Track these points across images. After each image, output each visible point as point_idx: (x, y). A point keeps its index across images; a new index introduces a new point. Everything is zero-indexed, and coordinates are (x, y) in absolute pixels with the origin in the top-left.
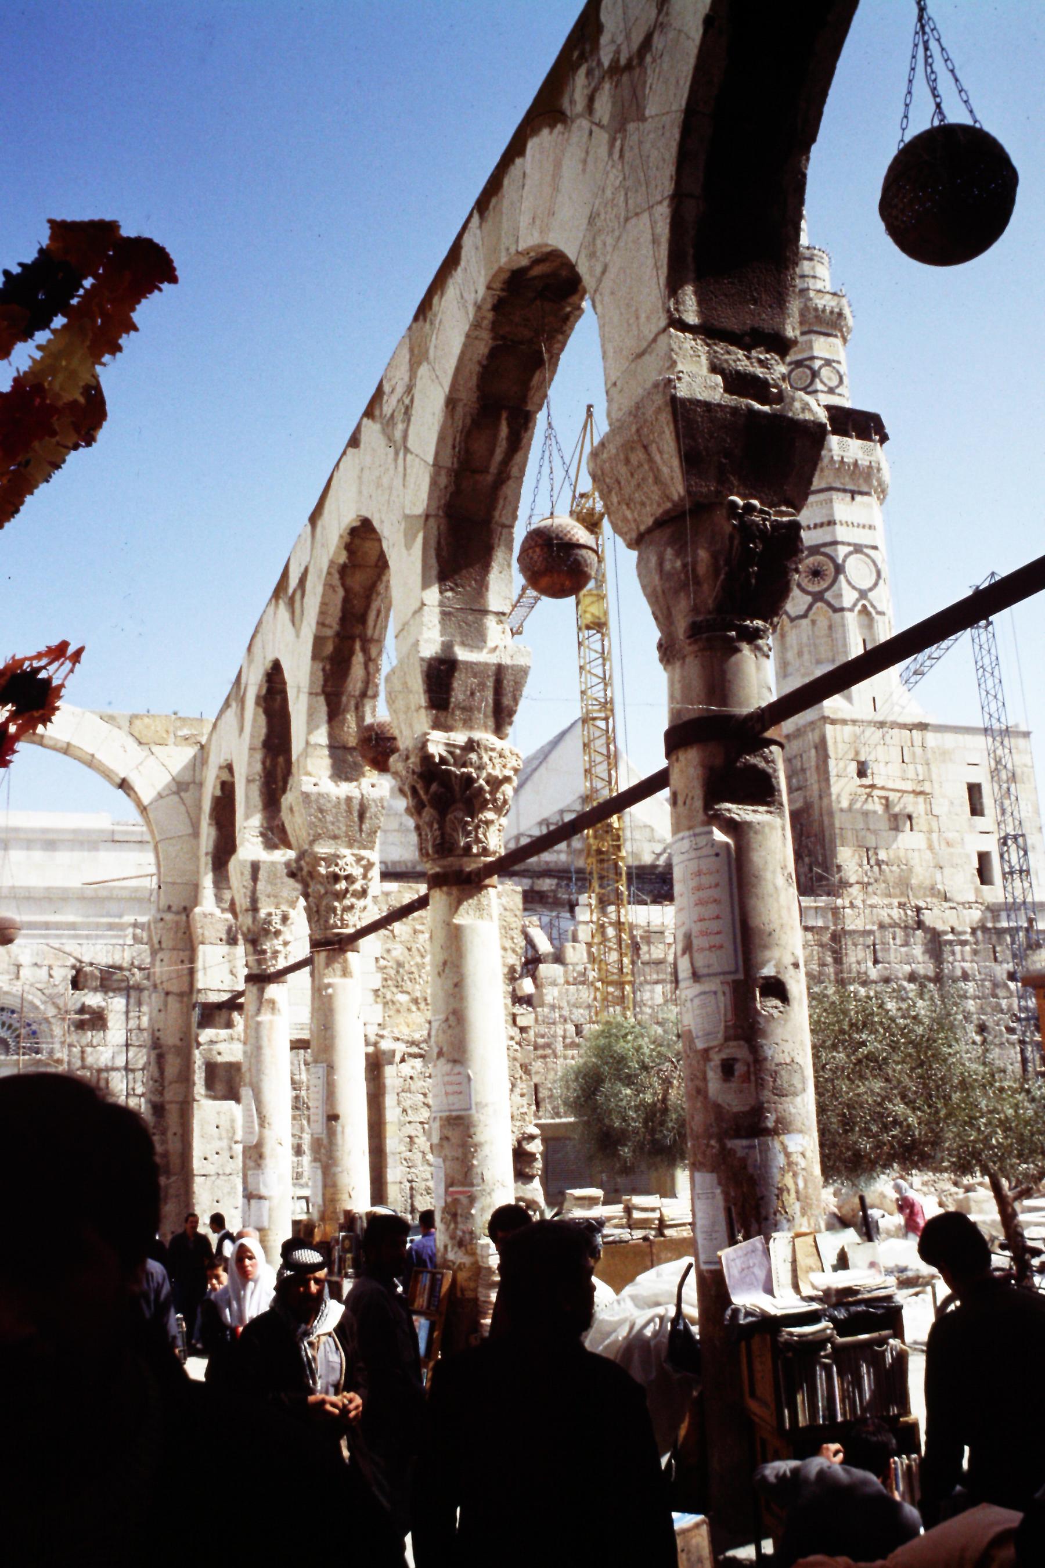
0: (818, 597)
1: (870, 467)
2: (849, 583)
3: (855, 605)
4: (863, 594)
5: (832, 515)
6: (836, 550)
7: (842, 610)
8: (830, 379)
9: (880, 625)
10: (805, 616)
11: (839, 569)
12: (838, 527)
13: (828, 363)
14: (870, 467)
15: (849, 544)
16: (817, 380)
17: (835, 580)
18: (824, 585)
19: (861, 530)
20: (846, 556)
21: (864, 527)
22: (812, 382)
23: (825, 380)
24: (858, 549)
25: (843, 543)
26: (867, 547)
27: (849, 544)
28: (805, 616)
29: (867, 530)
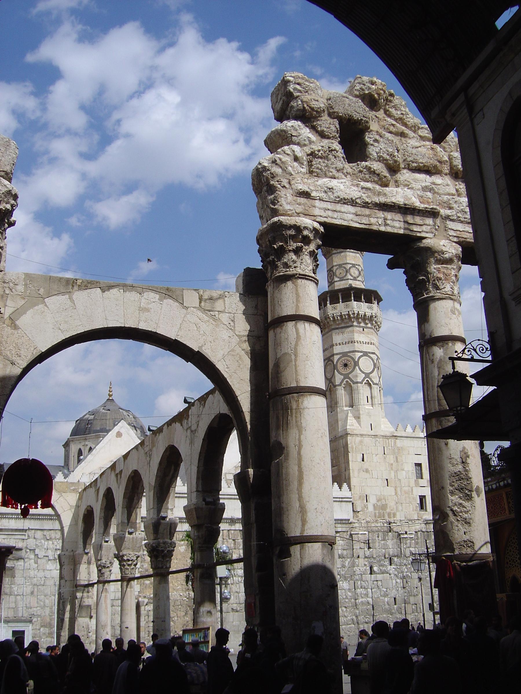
0: (346, 376)
1: (372, 316)
2: (360, 369)
3: (363, 380)
4: (367, 375)
5: (354, 338)
6: (354, 355)
7: (357, 383)
8: (354, 273)
9: (375, 389)
11: (356, 364)
12: (356, 344)
13: (354, 265)
15: (361, 352)
16: (348, 274)
17: (354, 368)
18: (348, 370)
20: (359, 358)
22: (346, 275)
23: (352, 274)
24: (366, 354)
25: (358, 352)
26: (369, 353)
27: (361, 352)
28: (340, 385)
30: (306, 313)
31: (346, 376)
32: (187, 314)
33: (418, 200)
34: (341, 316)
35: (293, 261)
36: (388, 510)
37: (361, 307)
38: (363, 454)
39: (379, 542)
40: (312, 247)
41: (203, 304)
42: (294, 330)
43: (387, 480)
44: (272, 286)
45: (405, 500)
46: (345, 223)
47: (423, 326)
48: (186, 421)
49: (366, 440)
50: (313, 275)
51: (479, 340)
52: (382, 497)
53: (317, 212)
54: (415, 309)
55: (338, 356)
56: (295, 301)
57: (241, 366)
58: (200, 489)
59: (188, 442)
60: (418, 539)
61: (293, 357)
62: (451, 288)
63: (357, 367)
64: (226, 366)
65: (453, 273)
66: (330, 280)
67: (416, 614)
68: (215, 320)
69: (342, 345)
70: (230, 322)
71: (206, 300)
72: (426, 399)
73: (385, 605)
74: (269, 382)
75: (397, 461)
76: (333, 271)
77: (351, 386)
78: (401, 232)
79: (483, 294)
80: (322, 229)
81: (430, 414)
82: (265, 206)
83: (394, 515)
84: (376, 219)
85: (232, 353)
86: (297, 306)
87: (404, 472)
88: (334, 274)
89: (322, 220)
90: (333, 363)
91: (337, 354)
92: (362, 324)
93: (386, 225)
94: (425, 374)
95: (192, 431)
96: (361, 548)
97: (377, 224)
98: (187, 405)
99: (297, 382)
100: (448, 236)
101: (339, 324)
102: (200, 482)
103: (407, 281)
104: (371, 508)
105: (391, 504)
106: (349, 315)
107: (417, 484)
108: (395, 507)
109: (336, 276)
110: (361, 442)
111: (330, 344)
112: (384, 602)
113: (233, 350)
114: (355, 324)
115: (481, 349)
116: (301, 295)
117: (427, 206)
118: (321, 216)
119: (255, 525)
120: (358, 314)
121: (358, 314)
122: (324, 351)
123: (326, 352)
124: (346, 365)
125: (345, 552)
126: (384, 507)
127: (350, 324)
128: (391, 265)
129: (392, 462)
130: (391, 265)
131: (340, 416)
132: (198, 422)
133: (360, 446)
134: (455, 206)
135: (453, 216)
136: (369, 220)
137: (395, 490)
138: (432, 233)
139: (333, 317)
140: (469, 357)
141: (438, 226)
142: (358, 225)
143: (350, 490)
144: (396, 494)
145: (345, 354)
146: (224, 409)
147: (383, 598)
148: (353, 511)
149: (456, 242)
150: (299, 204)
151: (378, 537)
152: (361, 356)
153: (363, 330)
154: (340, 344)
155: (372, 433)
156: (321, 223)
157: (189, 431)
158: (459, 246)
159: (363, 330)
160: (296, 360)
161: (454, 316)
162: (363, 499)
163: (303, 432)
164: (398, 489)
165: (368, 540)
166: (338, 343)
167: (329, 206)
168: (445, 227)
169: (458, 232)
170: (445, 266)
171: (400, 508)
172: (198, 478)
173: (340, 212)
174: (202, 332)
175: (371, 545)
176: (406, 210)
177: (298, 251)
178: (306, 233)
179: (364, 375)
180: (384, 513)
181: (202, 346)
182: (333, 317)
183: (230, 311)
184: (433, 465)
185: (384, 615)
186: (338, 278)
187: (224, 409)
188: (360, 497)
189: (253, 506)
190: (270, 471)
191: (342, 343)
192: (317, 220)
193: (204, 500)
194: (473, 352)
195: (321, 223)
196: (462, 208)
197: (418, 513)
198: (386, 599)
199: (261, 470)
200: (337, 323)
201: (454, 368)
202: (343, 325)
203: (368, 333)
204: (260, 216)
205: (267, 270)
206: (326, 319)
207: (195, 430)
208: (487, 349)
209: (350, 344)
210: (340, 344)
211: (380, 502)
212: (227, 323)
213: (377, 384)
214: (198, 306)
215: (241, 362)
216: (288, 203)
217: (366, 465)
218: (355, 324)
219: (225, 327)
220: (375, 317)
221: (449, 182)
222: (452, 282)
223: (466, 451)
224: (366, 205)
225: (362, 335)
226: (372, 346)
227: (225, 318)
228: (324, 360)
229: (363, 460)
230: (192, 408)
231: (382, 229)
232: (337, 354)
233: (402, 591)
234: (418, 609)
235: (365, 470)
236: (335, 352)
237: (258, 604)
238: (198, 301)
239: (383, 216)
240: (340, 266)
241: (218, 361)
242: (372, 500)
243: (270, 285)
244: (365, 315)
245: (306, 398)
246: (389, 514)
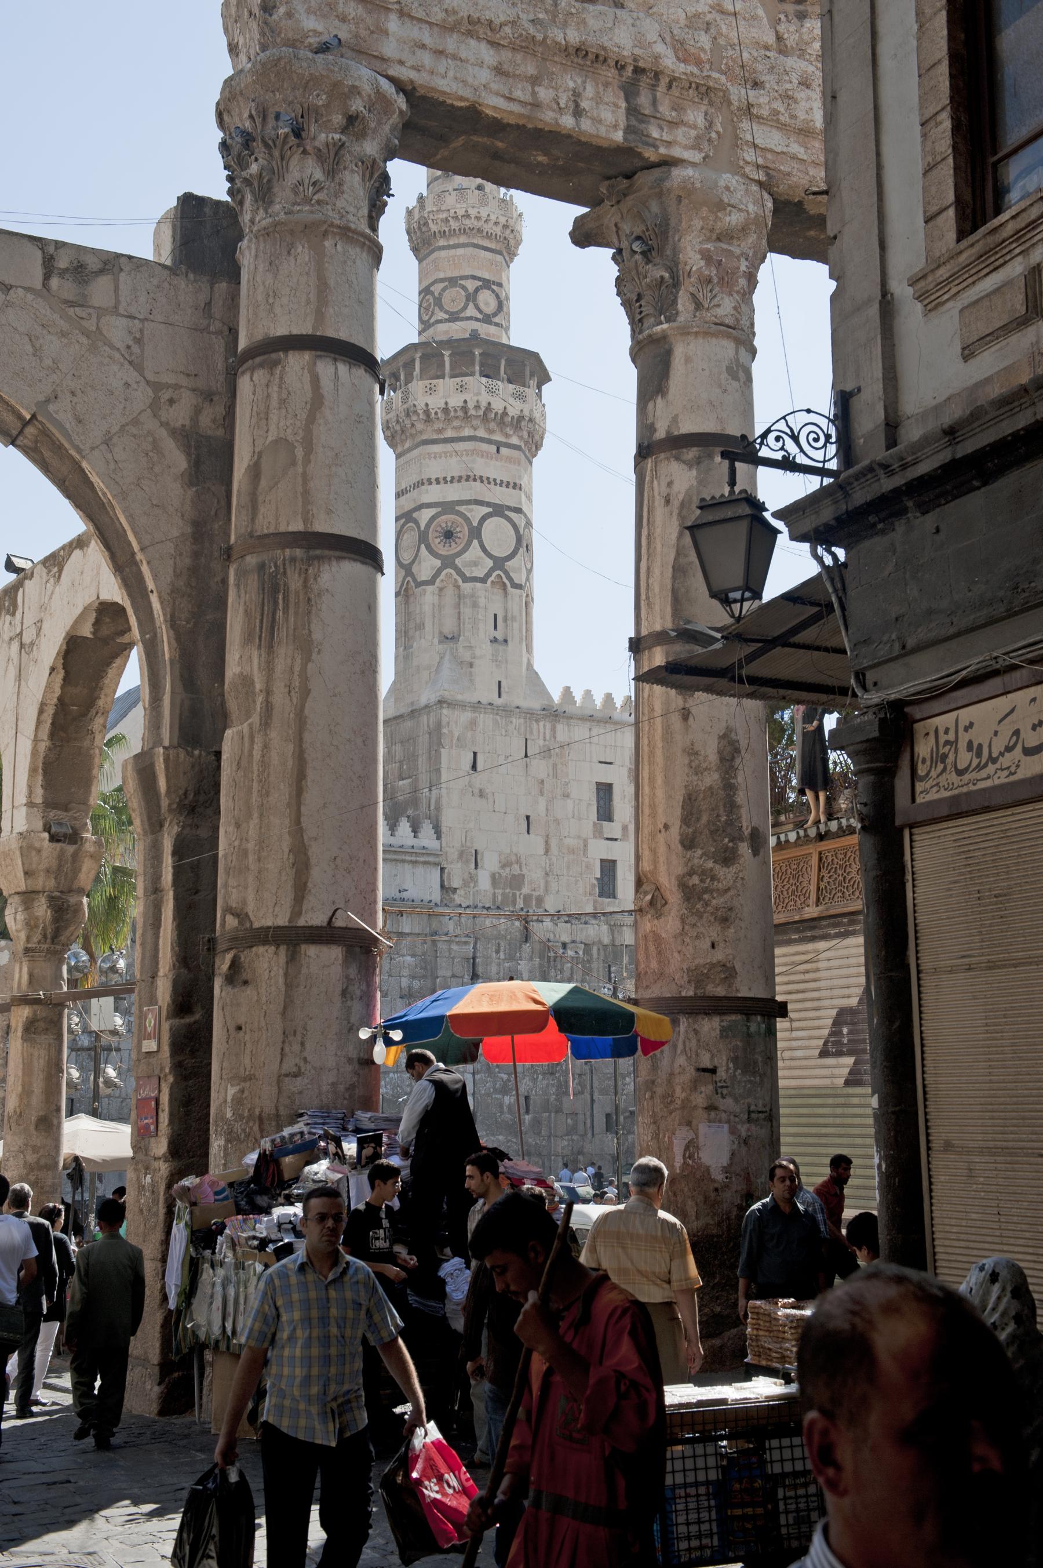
0: (448, 562)
1: (521, 418)
3: (488, 575)
4: (499, 563)
8: (487, 304)
10: (431, 582)
11: (476, 533)
18: (455, 548)
19: (504, 489)
20: (484, 519)
21: (508, 485)
23: (482, 306)
24: (499, 510)
26: (509, 508)
27: (488, 504)
28: (431, 582)
29: (510, 490)
30: (343, 335)
31: (448, 562)
32: (8, 304)
33: (670, 53)
34: (446, 410)
35: (314, 184)
36: (525, 890)
38: (475, 754)
39: (499, 964)
40: (370, 148)
41: (55, 282)
42: (307, 378)
43: (528, 817)
44: (253, 252)
45: (568, 868)
46: (467, 93)
47: (651, 405)
48: (8, 618)
49: (485, 720)
50: (368, 231)
51: (809, 411)
52: (514, 858)
53: (389, 48)
54: (634, 361)
55: (431, 512)
56: (313, 297)
57: (157, 469)
58: (39, 800)
59: (12, 672)
60: (589, 961)
61: (299, 453)
62: (735, 308)
63: (475, 542)
64: (112, 466)
65: (743, 268)
66: (426, 318)
67: (575, 1138)
68: (87, 334)
69: (442, 485)
70: (131, 343)
71: (66, 270)
72: (643, 597)
73: (502, 1112)
74: (230, 520)
75: (555, 776)
76: (432, 293)
77: (458, 587)
78: (619, 136)
79: (833, 285)
80: (401, 102)
81: (650, 635)
82: (246, 13)
83: (540, 900)
84: (551, 93)
85: (134, 430)
86: (320, 316)
87: (569, 802)
88: (438, 302)
89: (405, 73)
90: (419, 527)
91: (429, 506)
93: (578, 112)
94: (645, 532)
95: (22, 646)
96: (454, 976)
97: (555, 106)
98: (13, 577)
99: (305, 521)
100: (741, 163)
102: (40, 778)
103: (619, 282)
104: (484, 882)
105: (534, 875)
106: (465, 409)
107: (598, 833)
108: (542, 885)
109: (441, 308)
110: (473, 723)
111: (415, 478)
112: (501, 1106)
113: (135, 422)
115: (812, 436)
116: (332, 283)
117: (696, 71)
118: (401, 63)
119: (171, 893)
122: (398, 495)
123: (403, 498)
124: (449, 535)
125: (416, 984)
126: (517, 881)
128: (583, 236)
129: (542, 775)
130: (583, 236)
132: (41, 621)
133: (469, 734)
134: (769, 79)
135: (759, 105)
136: (534, 94)
137: (546, 842)
138: (700, 150)
139: (427, 412)
140: (778, 456)
141: (717, 133)
142: (501, 103)
143: (439, 838)
144: (547, 851)
145: (447, 507)
146: (113, 591)
147: (499, 1096)
148: (442, 886)
149: (760, 183)
150: (343, 19)
151: (498, 952)
152: (488, 516)
153: (498, 451)
155: (498, 702)
156: (399, 85)
157: (15, 646)
158: (766, 196)
159: (498, 451)
160: (307, 461)
161: (735, 384)
162: (468, 861)
163: (314, 656)
164: (553, 843)
165: (474, 958)
166: (433, 477)
167: (426, 37)
168: (737, 137)
169: (769, 156)
170: (725, 246)
171: (554, 886)
172: (33, 770)
173: (455, 57)
174: (48, 362)
175: (480, 970)
176: (637, 77)
177: (332, 159)
178: (357, 105)
179: (490, 563)
180: (514, 895)
181: (48, 401)
183: (132, 310)
184: (646, 767)
185: (501, 1138)
186: (446, 312)
187: (113, 591)
188: (461, 854)
189: (168, 845)
190: (218, 754)
191: (445, 478)
192: (391, 72)
193: (47, 828)
194: (791, 446)
195: (399, 85)
196: (788, 86)
197: (595, 902)
198: (507, 1100)
199: (197, 752)
200: (436, 426)
201: (732, 483)
202: (449, 434)
203: (509, 459)
204: (229, 45)
205: (241, 203)
206: (408, 415)
207: (32, 644)
208: (828, 437)
209: (463, 483)
211: (507, 870)
212: (118, 345)
213: (519, 587)
214: (38, 285)
215: (155, 459)
216: (309, 11)
217: (479, 780)
219: (117, 355)
220: (531, 420)
221: (760, 12)
222: (738, 292)
223: (733, 736)
224: (527, 46)
225: (493, 462)
226: (517, 491)
227: (117, 330)
228: (397, 519)
229: (474, 767)
230: (27, 582)
231: (568, 121)
232: (429, 506)
233: (545, 1082)
234: (581, 1127)
235: (477, 791)
236: (426, 499)
237: (165, 1099)
238: (38, 272)
239: (571, 84)
241: (92, 449)
242: (490, 863)
243: (249, 247)
244: (505, 413)
245: (326, 567)
246: (527, 899)
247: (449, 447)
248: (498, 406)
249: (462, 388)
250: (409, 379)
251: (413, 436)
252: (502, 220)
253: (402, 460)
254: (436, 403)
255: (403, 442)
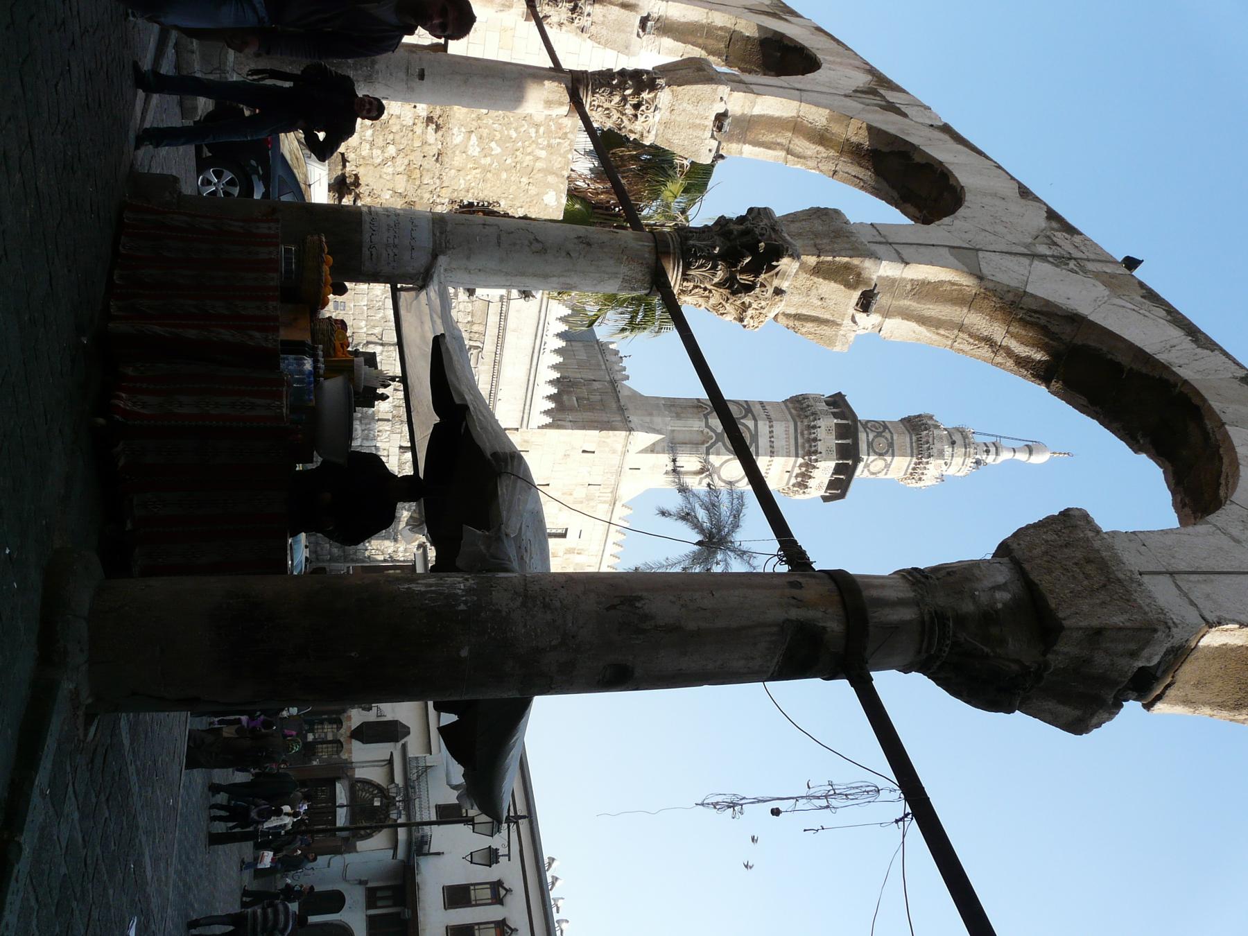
1: (806, 487)
7: (708, 454)
13: (888, 466)
14: (806, 487)
22: (876, 453)
28: (707, 426)
34: (815, 440)
37: (824, 470)
49: (615, 460)
77: (703, 443)
88: (879, 435)
91: (756, 426)
92: (797, 471)
101: (802, 434)
106: (816, 452)
109: (875, 437)
110: (614, 452)
111: (773, 416)
114: (800, 460)
120: (814, 467)
121: (814, 467)
122: (761, 403)
123: (759, 407)
127: (800, 452)
131: (658, 421)
139: (814, 427)
154: (771, 432)
182: (814, 427)
202: (800, 441)
206: (813, 414)
210: (771, 432)
218: (800, 460)
229: (584, 451)
232: (756, 426)
236: (760, 423)
240: (891, 445)
244: (810, 477)
247: (792, 441)
248: (815, 473)
249: (829, 451)
250: (835, 415)
251: (799, 416)
252: (924, 477)
253: (783, 407)
254: (821, 433)
255: (795, 409)
